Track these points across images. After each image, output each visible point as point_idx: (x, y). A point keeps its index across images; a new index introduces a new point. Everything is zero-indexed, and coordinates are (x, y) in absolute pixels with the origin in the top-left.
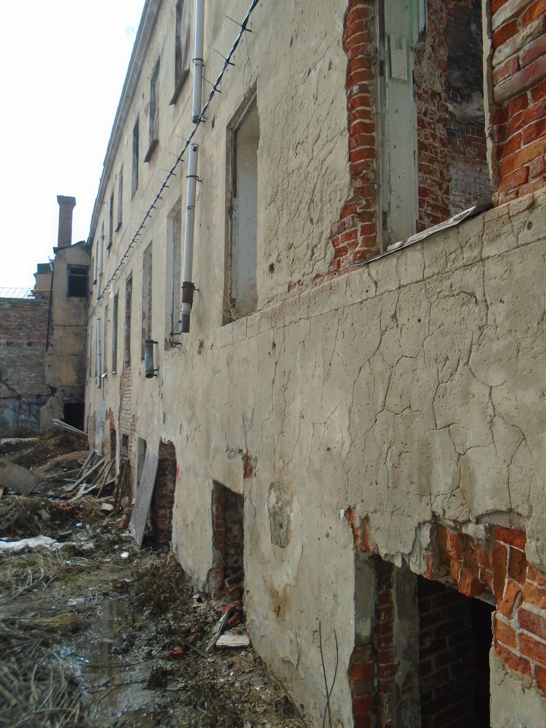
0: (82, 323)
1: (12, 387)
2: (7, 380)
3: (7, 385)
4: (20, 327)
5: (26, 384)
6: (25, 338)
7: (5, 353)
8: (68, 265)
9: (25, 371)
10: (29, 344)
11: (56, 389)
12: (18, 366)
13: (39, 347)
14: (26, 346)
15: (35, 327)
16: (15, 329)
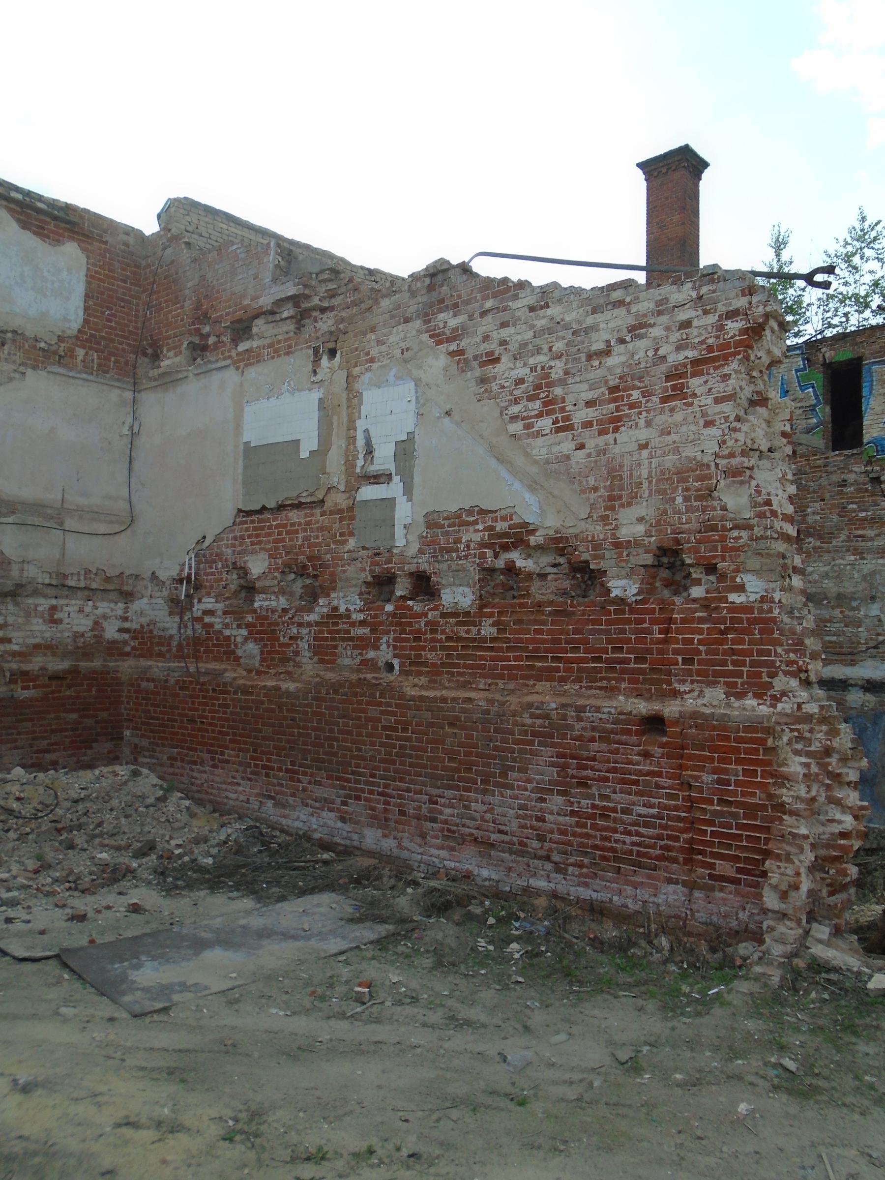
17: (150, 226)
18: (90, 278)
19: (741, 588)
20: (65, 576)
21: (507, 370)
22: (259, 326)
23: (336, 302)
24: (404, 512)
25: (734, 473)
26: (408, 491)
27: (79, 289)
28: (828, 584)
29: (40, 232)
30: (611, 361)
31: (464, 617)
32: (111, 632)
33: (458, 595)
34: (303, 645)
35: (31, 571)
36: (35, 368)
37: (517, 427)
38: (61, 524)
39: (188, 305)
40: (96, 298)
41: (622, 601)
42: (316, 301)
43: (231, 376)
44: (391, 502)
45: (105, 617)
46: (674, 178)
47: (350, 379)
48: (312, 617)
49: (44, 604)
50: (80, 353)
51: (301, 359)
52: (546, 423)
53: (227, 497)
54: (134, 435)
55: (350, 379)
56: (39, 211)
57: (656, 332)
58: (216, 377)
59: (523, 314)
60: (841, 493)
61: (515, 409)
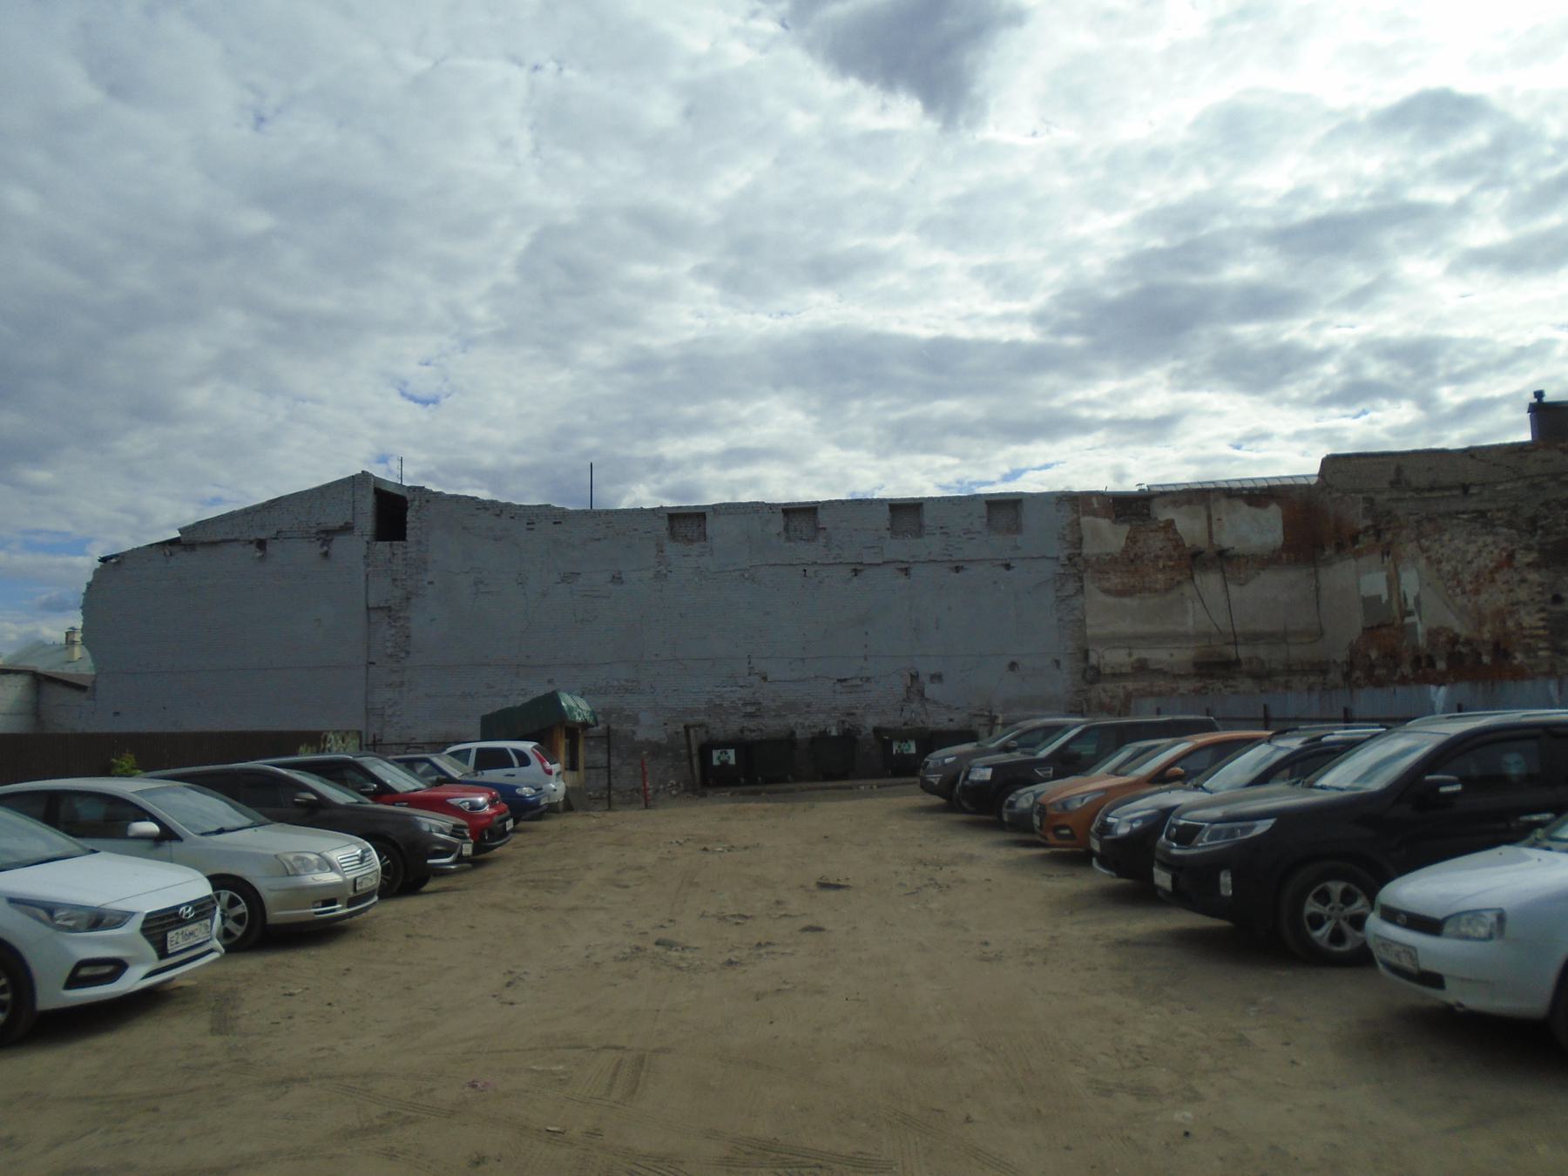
21: (1446, 567)
22: (1361, 537)
24: (1420, 629)
27: (1280, 525)
30: (1474, 565)
40: (1288, 526)
43: (1353, 562)
44: (1414, 625)
47: (1396, 567)
49: (1282, 680)
50: (1284, 556)
54: (1318, 589)
55: (1396, 567)
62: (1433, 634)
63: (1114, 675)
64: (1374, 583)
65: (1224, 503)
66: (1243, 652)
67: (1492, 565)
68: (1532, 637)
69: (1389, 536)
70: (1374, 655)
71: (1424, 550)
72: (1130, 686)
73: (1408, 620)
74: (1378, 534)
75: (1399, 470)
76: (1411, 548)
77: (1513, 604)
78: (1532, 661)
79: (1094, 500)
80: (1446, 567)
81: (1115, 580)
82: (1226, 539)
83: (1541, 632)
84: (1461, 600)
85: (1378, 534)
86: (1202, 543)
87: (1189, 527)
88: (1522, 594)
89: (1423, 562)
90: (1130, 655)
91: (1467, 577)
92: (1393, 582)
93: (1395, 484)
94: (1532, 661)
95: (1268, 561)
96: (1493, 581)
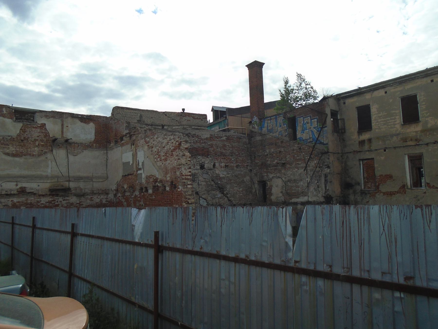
0: (340, 152)
1: (230, 199)
2: (227, 194)
3: (227, 197)
4: (232, 154)
5: (237, 196)
6: (234, 162)
7: (225, 173)
8: (331, 110)
9: (236, 187)
10: (237, 166)
11: (332, 198)
12: (232, 183)
13: (242, 169)
14: (235, 168)
15: (239, 154)
16: (229, 155)
17: (109, 114)
18: (96, 129)
19: (179, 188)
20: (93, 191)
21: (155, 149)
22: (124, 138)
23: (136, 133)
24: (143, 176)
25: (178, 168)
26: (144, 172)
27: (94, 132)
28: (292, 177)
29: (85, 122)
30: (165, 148)
31: (151, 195)
32: (104, 201)
33: (150, 191)
34: (132, 202)
35: (87, 190)
36: (85, 150)
37: (156, 160)
38: (92, 180)
39: (114, 133)
41: (167, 191)
42: (132, 133)
44: (141, 174)
45: (103, 198)
46: (256, 69)
47: (136, 150)
48: (133, 197)
49: (89, 197)
50: (95, 145)
51: (129, 146)
52: (159, 159)
53: (121, 173)
54: (107, 160)
55: (136, 150)
56: (84, 118)
57: (170, 144)
58: (118, 148)
59: (156, 139)
60: (293, 152)
61: (155, 157)
62: (148, 177)
63: (7, 195)
64: (128, 157)
65: (70, 119)
66: (72, 185)
67: (172, 148)
68: (186, 179)
69: (134, 138)
70: (126, 187)
71: (147, 142)
72: (15, 200)
73: (139, 172)
74: (131, 136)
75: (141, 116)
76: (142, 142)
77: (179, 165)
78: (185, 190)
79: (4, 110)
80: (155, 149)
81: (12, 149)
82: (69, 135)
83: (189, 177)
84: (159, 163)
85: (131, 136)
86: (58, 135)
87: (53, 128)
88: (183, 161)
89: (146, 147)
90: (17, 185)
91: (162, 154)
92: (135, 156)
93: (139, 121)
94: (185, 190)
95: (88, 146)
96: (172, 155)
